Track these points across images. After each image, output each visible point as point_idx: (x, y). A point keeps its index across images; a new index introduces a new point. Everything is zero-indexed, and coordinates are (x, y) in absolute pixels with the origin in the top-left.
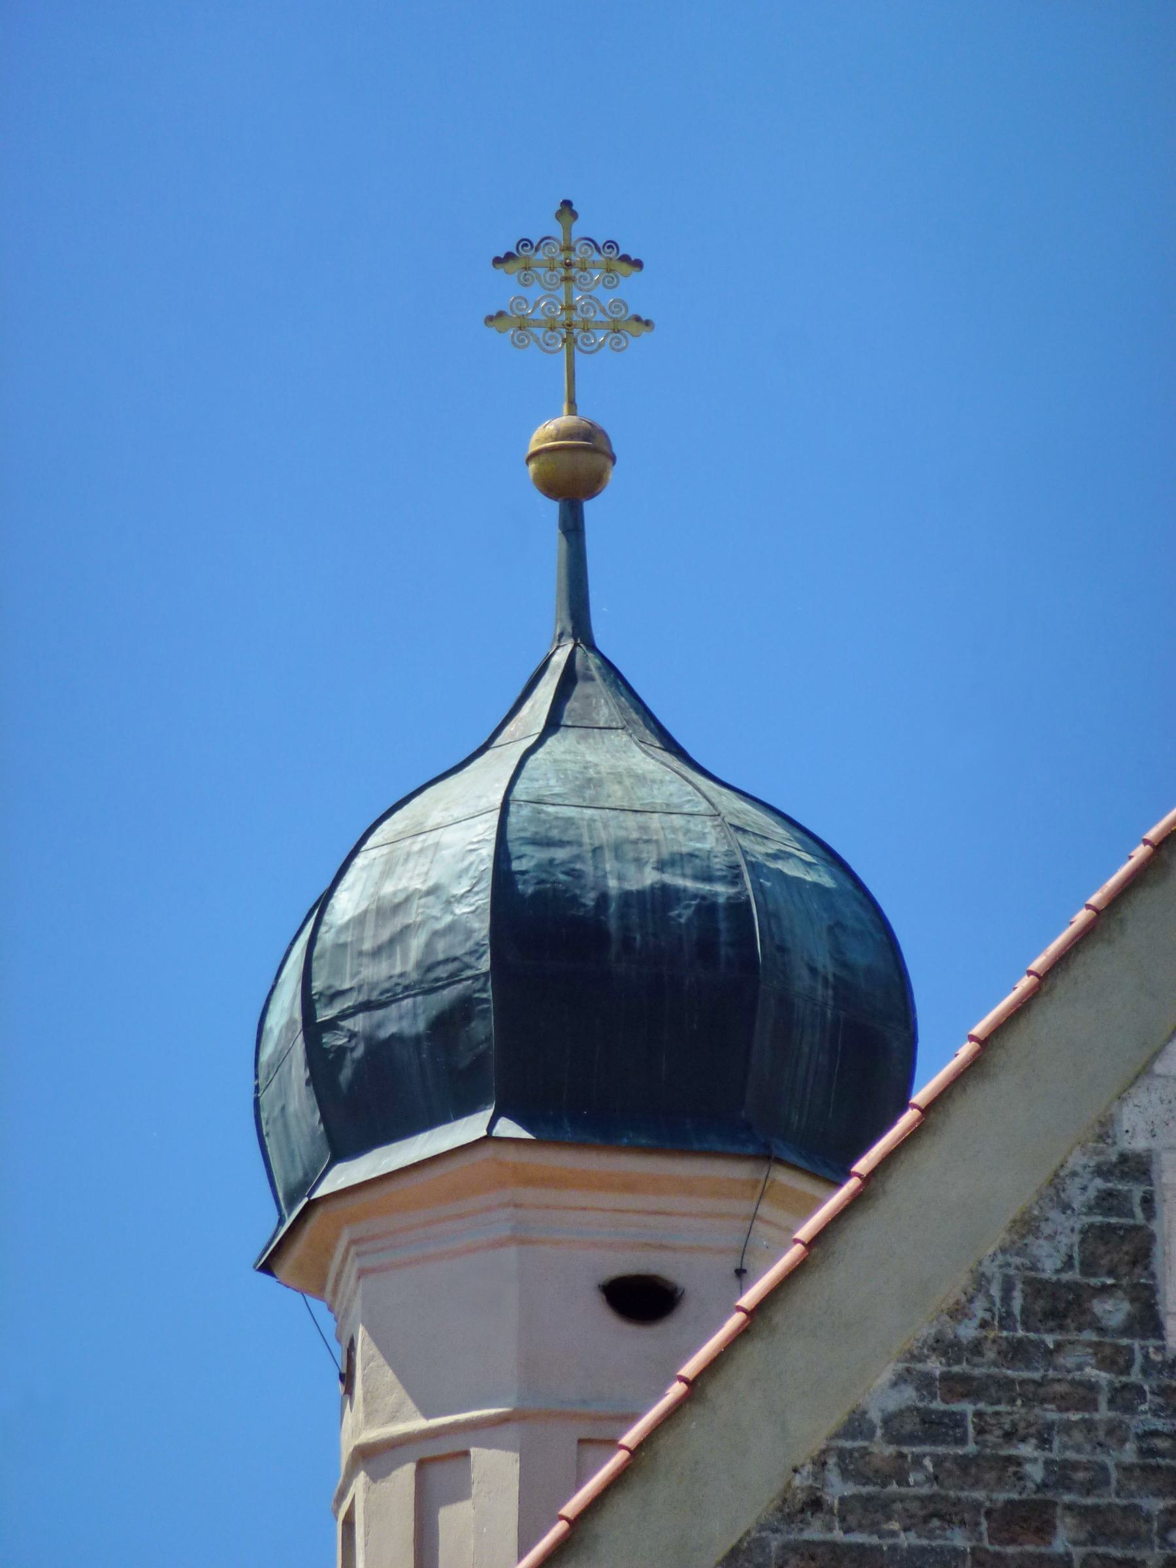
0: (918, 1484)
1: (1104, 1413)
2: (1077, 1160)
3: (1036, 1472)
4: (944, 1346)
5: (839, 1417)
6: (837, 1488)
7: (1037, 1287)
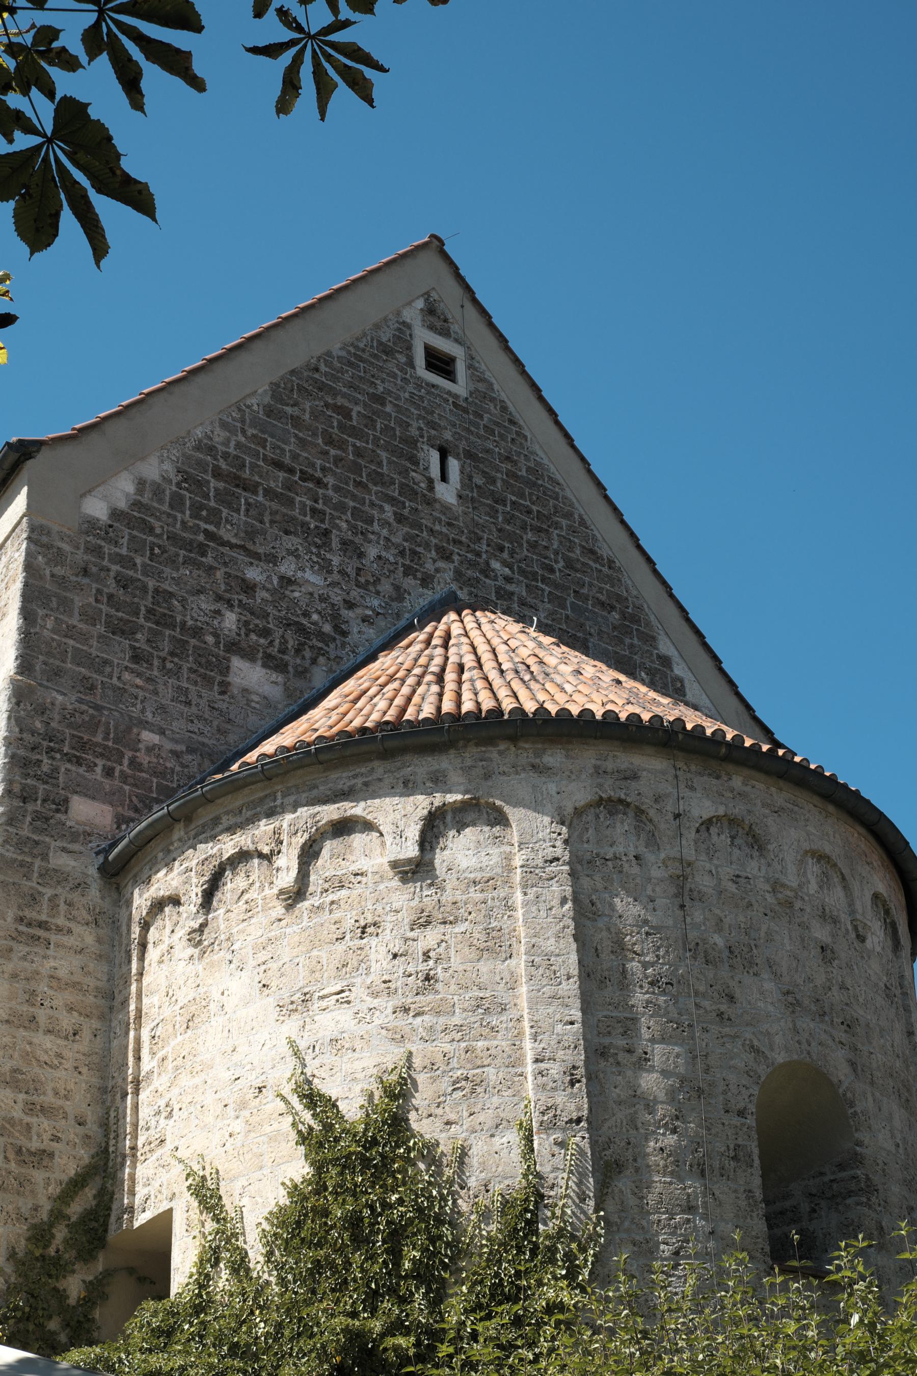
1: (399, 382)
2: (391, 316)
7: (380, 343)
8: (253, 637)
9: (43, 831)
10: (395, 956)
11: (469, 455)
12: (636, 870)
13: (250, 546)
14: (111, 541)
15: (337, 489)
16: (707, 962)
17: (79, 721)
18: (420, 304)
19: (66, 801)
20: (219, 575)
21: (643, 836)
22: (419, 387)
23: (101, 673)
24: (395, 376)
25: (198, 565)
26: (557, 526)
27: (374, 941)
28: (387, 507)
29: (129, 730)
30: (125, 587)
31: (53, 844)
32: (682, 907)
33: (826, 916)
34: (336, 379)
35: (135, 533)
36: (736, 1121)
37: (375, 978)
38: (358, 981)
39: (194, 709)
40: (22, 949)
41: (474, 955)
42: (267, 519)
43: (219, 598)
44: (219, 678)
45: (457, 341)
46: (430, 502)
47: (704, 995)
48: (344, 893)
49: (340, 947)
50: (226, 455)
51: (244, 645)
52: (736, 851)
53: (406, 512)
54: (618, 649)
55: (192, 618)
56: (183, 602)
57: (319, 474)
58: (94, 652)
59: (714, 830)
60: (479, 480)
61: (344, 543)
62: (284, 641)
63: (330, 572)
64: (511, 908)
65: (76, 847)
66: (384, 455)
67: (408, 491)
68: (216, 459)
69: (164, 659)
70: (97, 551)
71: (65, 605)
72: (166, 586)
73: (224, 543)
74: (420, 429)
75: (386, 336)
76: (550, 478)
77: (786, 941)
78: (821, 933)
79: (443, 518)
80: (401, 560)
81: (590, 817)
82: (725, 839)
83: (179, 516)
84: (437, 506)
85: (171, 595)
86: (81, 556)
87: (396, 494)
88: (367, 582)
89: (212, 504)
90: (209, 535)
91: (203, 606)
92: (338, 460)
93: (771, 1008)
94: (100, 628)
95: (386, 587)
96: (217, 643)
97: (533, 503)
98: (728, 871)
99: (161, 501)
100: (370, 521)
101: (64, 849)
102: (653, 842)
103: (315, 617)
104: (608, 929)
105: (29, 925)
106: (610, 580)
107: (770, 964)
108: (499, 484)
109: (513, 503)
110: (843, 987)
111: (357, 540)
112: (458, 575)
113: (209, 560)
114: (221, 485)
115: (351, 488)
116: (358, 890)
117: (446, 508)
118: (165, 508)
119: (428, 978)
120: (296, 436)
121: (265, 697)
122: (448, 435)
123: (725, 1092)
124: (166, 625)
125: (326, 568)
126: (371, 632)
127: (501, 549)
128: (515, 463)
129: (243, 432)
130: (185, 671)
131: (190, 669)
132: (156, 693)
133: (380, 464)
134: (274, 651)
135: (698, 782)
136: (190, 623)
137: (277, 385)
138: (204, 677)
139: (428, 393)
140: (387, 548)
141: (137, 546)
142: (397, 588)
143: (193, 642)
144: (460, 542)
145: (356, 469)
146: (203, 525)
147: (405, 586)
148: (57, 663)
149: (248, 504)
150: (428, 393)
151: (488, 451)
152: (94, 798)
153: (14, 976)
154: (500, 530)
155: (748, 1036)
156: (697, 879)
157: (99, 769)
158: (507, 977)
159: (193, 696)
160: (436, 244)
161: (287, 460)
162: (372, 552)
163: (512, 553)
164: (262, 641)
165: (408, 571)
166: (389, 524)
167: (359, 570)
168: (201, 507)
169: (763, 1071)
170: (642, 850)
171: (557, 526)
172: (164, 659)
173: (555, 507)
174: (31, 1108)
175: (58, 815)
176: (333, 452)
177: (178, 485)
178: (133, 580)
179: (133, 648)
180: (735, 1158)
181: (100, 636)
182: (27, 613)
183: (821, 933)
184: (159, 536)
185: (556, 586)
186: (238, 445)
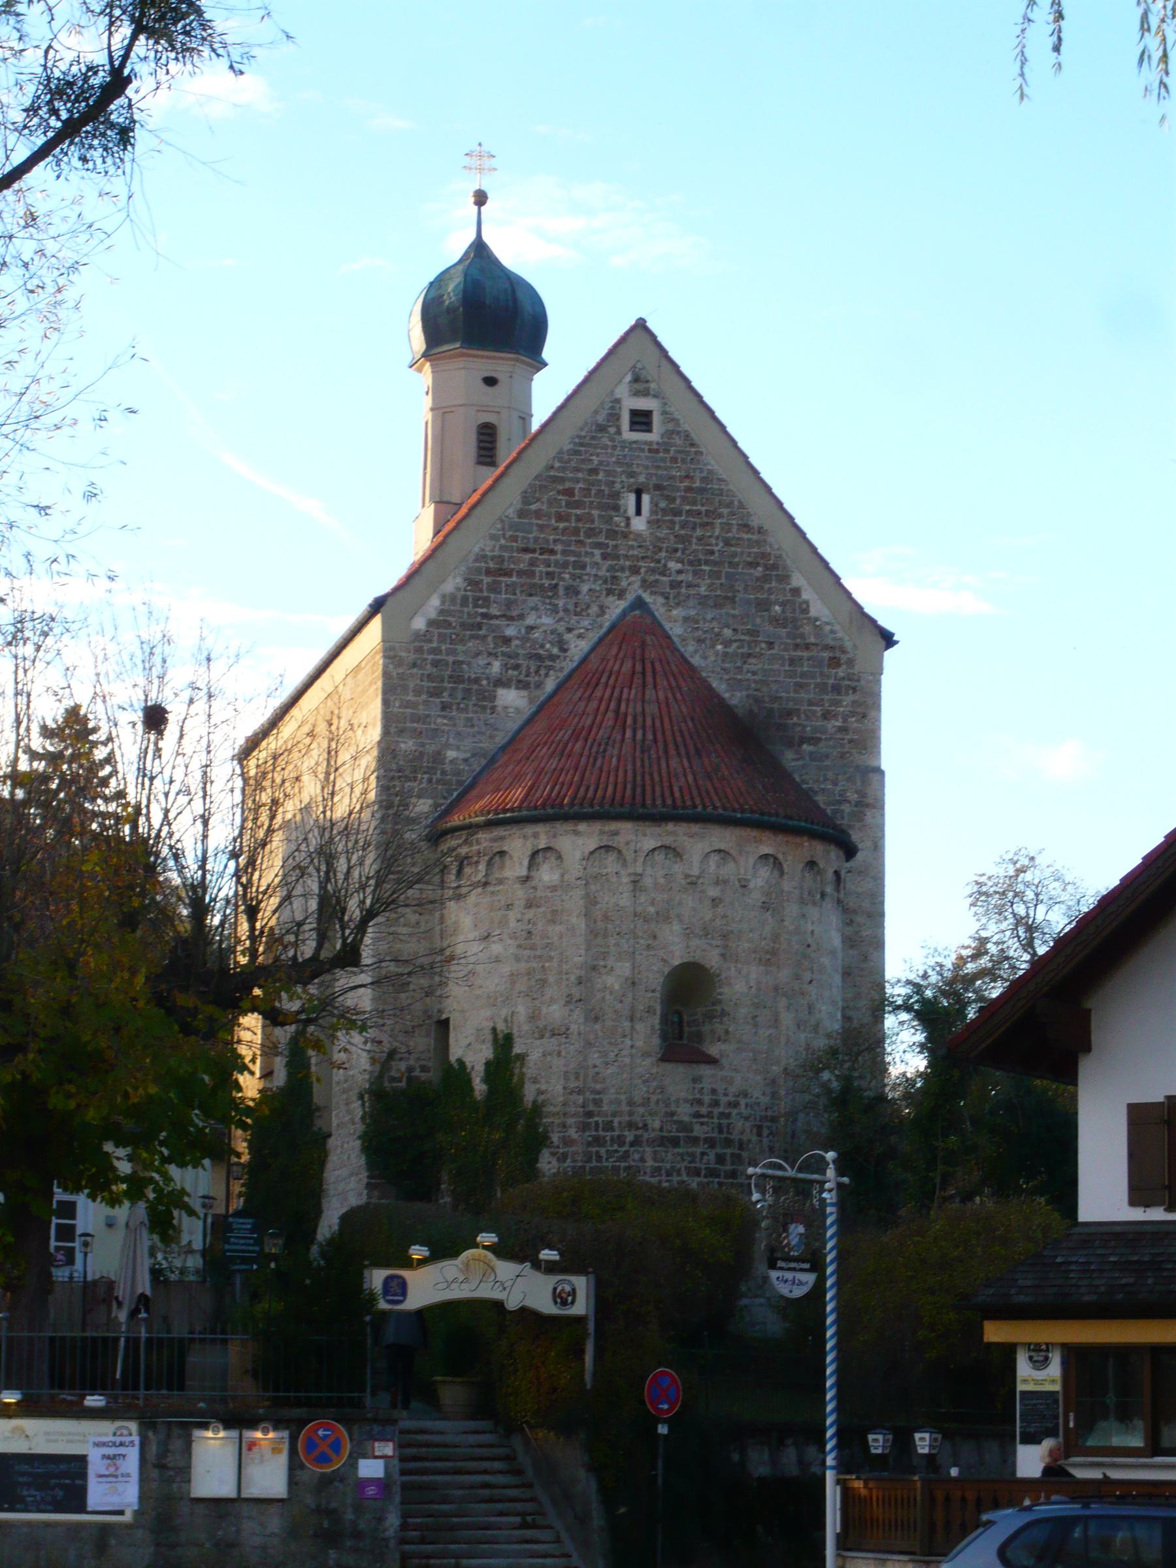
0: (573, 464)
1: (609, 451)
3: (596, 462)
4: (579, 437)
6: (557, 465)
8: (510, 672)
11: (658, 487)
13: (508, 613)
15: (564, 552)
20: (490, 639)
23: (424, 723)
24: (605, 447)
26: (720, 516)
35: (441, 631)
39: (476, 729)
42: (518, 592)
43: (490, 654)
45: (655, 396)
50: (493, 558)
51: (504, 679)
53: (609, 550)
54: (759, 595)
56: (469, 664)
58: (421, 712)
60: (663, 504)
61: (567, 588)
62: (528, 668)
63: (557, 612)
66: (595, 513)
67: (612, 534)
68: (486, 562)
69: (459, 704)
70: (419, 650)
71: (405, 688)
72: (460, 658)
75: (601, 419)
76: (720, 480)
79: (635, 544)
83: (466, 610)
84: (632, 536)
85: (462, 662)
86: (412, 656)
88: (582, 610)
89: (485, 594)
90: (484, 615)
92: (565, 529)
94: (424, 697)
95: (594, 609)
100: (583, 567)
103: (548, 646)
108: (678, 502)
109: (688, 511)
111: (575, 584)
112: (645, 584)
114: (490, 579)
115: (572, 548)
117: (638, 535)
118: (458, 608)
120: (537, 525)
122: (642, 479)
125: (555, 610)
129: (504, 535)
131: (475, 705)
132: (455, 725)
133: (593, 522)
134: (522, 677)
136: (473, 676)
137: (526, 492)
141: (442, 638)
143: (475, 687)
144: (646, 557)
146: (481, 610)
147: (607, 604)
149: (507, 585)
150: (631, 449)
151: (672, 478)
159: (475, 722)
161: (531, 546)
162: (585, 588)
163: (683, 553)
164: (516, 673)
165: (609, 592)
166: (597, 564)
167: (576, 605)
171: (720, 516)
172: (459, 704)
176: (562, 525)
177: (466, 590)
178: (441, 661)
181: (424, 701)
182: (386, 703)
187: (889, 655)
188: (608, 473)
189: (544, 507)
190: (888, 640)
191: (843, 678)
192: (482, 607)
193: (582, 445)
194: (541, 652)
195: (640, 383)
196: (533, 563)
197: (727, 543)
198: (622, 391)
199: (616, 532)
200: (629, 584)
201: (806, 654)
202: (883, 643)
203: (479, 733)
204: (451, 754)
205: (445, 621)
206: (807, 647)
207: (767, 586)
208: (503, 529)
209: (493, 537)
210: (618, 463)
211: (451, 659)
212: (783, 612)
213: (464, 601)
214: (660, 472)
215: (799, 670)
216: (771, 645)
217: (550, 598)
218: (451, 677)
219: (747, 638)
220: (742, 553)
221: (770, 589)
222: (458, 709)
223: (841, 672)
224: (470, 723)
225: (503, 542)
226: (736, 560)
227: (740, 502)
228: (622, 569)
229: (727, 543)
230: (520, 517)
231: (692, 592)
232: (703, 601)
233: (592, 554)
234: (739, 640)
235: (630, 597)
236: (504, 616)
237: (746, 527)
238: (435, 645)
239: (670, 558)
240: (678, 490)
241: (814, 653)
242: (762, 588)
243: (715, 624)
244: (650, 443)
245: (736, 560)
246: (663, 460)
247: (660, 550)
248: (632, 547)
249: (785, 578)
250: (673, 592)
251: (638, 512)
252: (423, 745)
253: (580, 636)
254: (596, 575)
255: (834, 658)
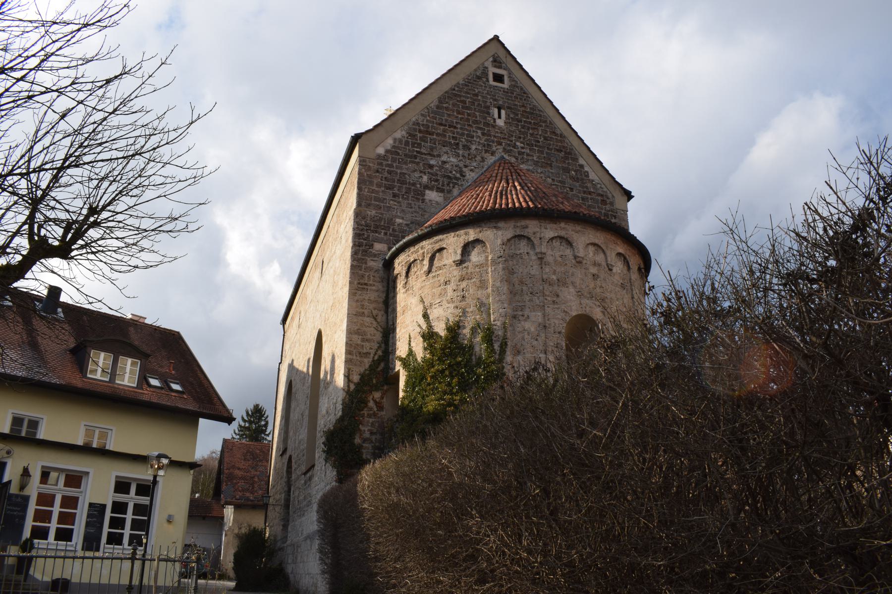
5: (456, 82)
7: (477, 76)
8: (433, 182)
9: (365, 255)
10: (454, 290)
11: (509, 108)
12: (527, 257)
13: (431, 153)
14: (385, 160)
15: (461, 128)
16: (550, 285)
17: (376, 219)
18: (491, 59)
19: (373, 245)
21: (530, 246)
22: (490, 88)
23: (383, 202)
24: (482, 86)
25: (414, 162)
26: (541, 126)
27: (449, 286)
28: (479, 131)
29: (392, 219)
30: (390, 174)
31: (368, 259)
32: (542, 268)
33: (595, 264)
34: (460, 91)
35: (394, 156)
36: (557, 335)
37: (448, 298)
38: (444, 299)
39: (413, 209)
40: (360, 292)
41: (476, 289)
42: (437, 143)
43: (421, 172)
44: (421, 198)
45: (504, 69)
46: (494, 126)
47: (548, 296)
48: (441, 271)
49: (440, 288)
50: (423, 125)
52: (562, 247)
53: (485, 132)
54: (563, 165)
55: (412, 180)
56: (409, 175)
57: (455, 125)
58: (381, 197)
59: (554, 241)
60: (512, 116)
61: (464, 146)
62: (443, 182)
63: (459, 157)
64: (487, 273)
65: (376, 259)
66: (477, 114)
67: (488, 125)
70: (381, 164)
71: (371, 183)
72: (403, 171)
73: (422, 154)
74: (491, 102)
77: (579, 275)
78: (593, 270)
80: (484, 148)
81: (512, 242)
82: (558, 243)
83: (408, 148)
84: (497, 127)
85: (405, 174)
86: (376, 167)
87: (482, 126)
88: (472, 158)
89: (419, 142)
91: (416, 176)
92: (461, 119)
93: (572, 297)
94: (383, 189)
95: (478, 158)
96: (421, 187)
97: (532, 120)
98: (558, 254)
99: (401, 144)
100: (473, 137)
101: (372, 260)
102: (533, 246)
103: (454, 172)
104: (517, 278)
105: (362, 285)
106: (561, 141)
107: (572, 283)
108: (519, 116)
109: (524, 121)
110: (601, 287)
111: (468, 144)
112: (504, 150)
113: (417, 160)
114: (421, 135)
116: (445, 270)
117: (500, 128)
118: (403, 146)
119: (463, 297)
120: (447, 113)
121: (437, 202)
122: (501, 103)
123: (554, 327)
124: (403, 184)
125: (457, 155)
126: (473, 174)
127: (520, 138)
128: (525, 107)
130: (410, 197)
131: (412, 197)
132: (401, 206)
133: (476, 117)
134: (440, 186)
135: (548, 226)
138: (417, 198)
139: (494, 89)
140: (478, 145)
141: (394, 160)
142: (482, 158)
143: (413, 188)
144: (505, 138)
145: (468, 120)
146: (416, 149)
148: (369, 202)
149: (431, 139)
150: (494, 89)
151: (516, 105)
152: (381, 243)
153: (357, 301)
154: (520, 132)
155: (563, 307)
156: (548, 257)
157: (382, 234)
158: (486, 295)
159: (413, 205)
160: (496, 38)
161: (444, 122)
162: (473, 147)
163: (524, 138)
164: (436, 183)
165: (486, 151)
166: (480, 137)
167: (469, 155)
168: (415, 143)
169: (568, 319)
170: (529, 251)
171: (541, 126)
173: (540, 119)
174: (363, 340)
175: (370, 250)
176: (460, 116)
177: (407, 138)
178: (393, 171)
179: (393, 193)
180: (557, 347)
181: (383, 191)
182: (359, 188)
183: (593, 270)
184: (401, 156)
185: (540, 147)
186: (427, 121)
187: (631, 205)
188: (483, 97)
189: (451, 106)
190: (629, 195)
191: (609, 211)
192: (417, 148)
193: (470, 83)
194: (450, 175)
195: (497, 62)
196: (444, 131)
197: (545, 138)
198: (488, 64)
199: (489, 124)
200: (497, 149)
201: (589, 196)
202: (626, 198)
203: (415, 212)
204: (399, 221)
205: (396, 152)
206: (590, 193)
207: (567, 162)
208: (429, 113)
209: (422, 115)
210: (488, 94)
211: (399, 171)
212: (576, 174)
213: (407, 143)
214: (509, 101)
215: (587, 203)
216: (572, 189)
217: (455, 149)
218: (398, 180)
219: (559, 184)
220: (553, 144)
221: (569, 163)
222: (403, 198)
223: (608, 207)
224: (410, 206)
225: (428, 118)
226: (551, 147)
227: (550, 121)
228: (493, 142)
229: (545, 138)
230: (437, 108)
231: (530, 158)
232: (536, 163)
233: (477, 132)
234: (556, 185)
235: (497, 156)
236: (429, 154)
237: (554, 133)
238: (390, 163)
239: (518, 141)
240: (519, 111)
241: (594, 196)
242: (565, 162)
243: (542, 175)
244: (504, 88)
245: (551, 147)
246: (511, 97)
247: (512, 136)
248: (497, 132)
249: (576, 160)
250: (520, 157)
251: (500, 117)
252: (382, 214)
253: (471, 170)
254: (479, 142)
255: (604, 200)
